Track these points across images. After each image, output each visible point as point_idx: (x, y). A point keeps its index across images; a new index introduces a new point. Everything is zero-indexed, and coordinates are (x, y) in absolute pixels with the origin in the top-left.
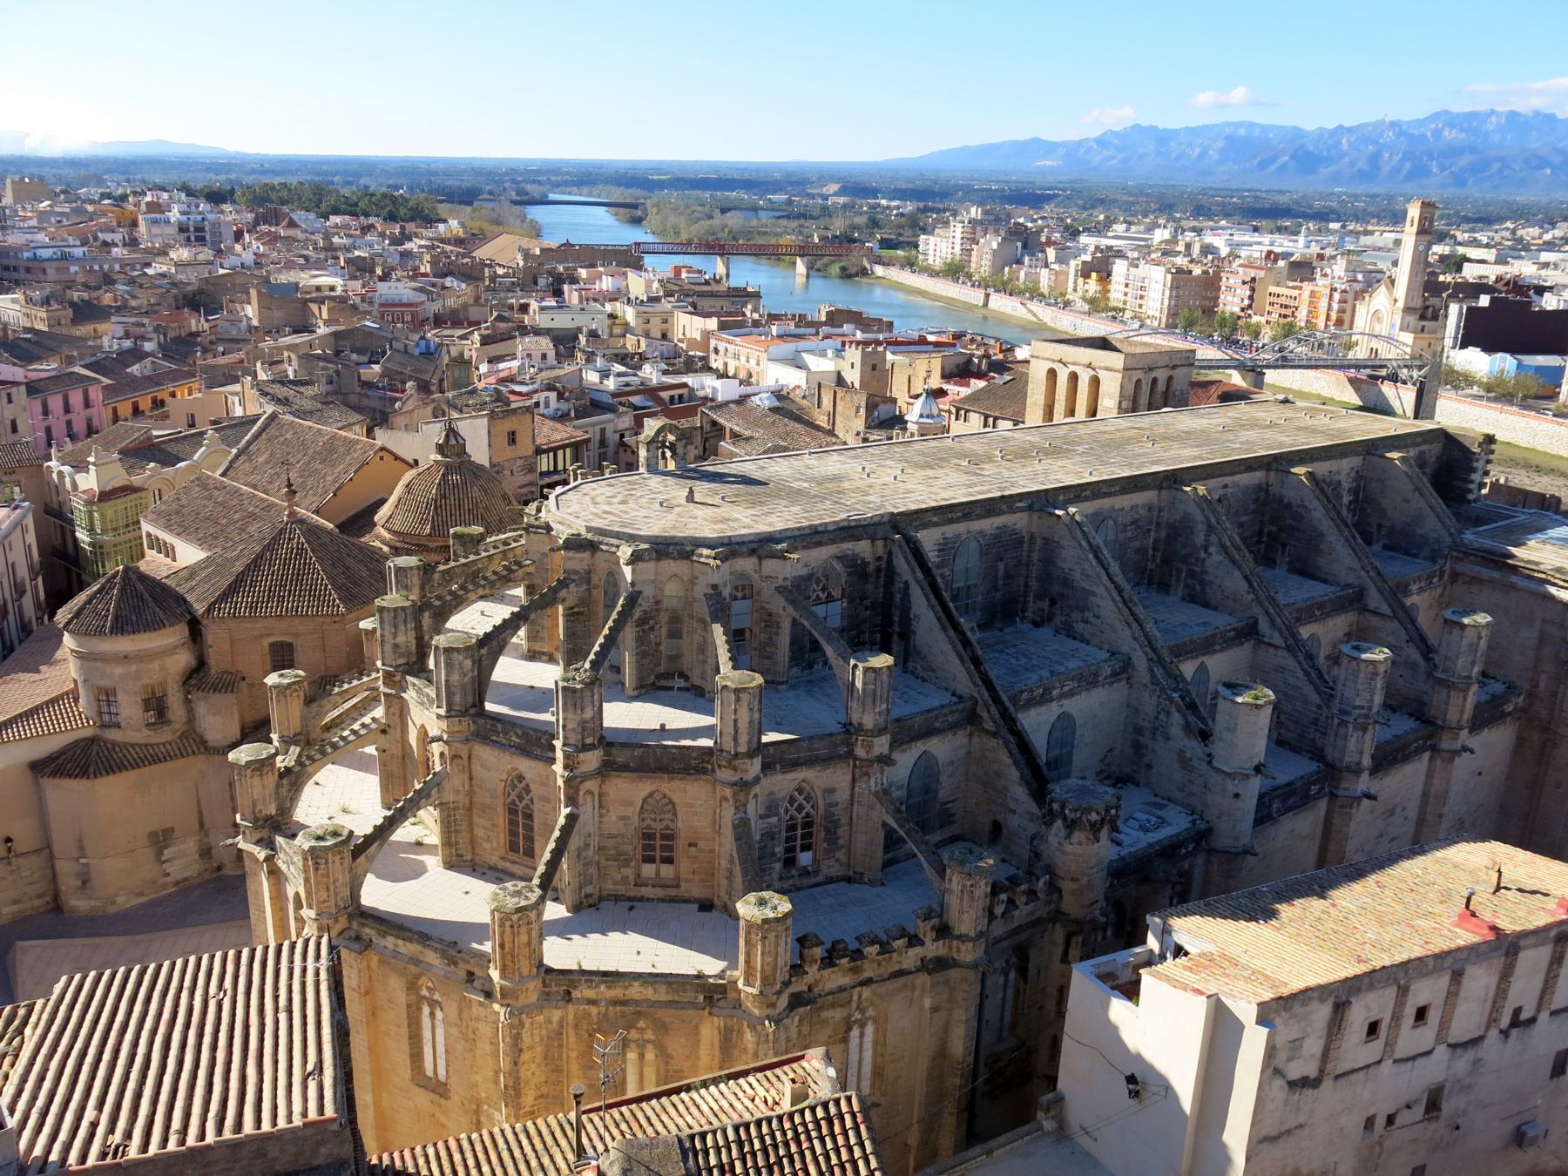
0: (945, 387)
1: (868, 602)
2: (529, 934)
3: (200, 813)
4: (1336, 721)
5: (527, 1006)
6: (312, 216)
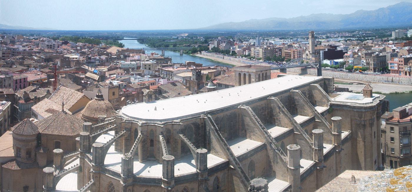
1: (200, 135)
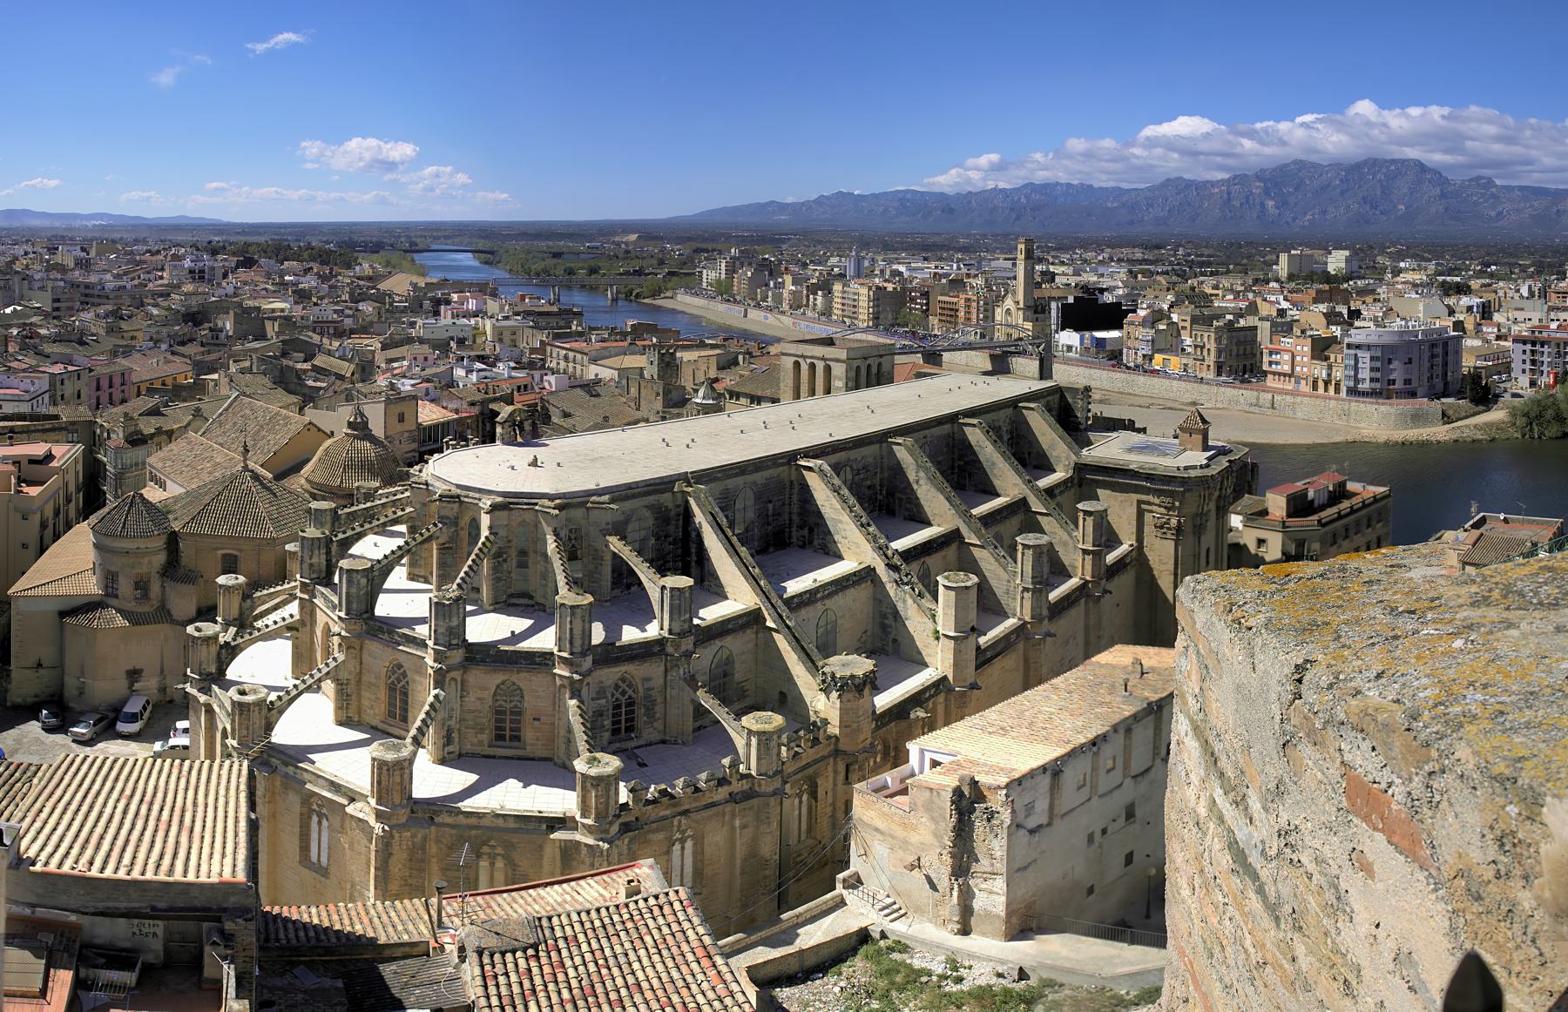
0: (720, 376)
2: (402, 776)
3: (162, 662)
4: (1020, 589)
5: (398, 825)
6: (272, 262)
